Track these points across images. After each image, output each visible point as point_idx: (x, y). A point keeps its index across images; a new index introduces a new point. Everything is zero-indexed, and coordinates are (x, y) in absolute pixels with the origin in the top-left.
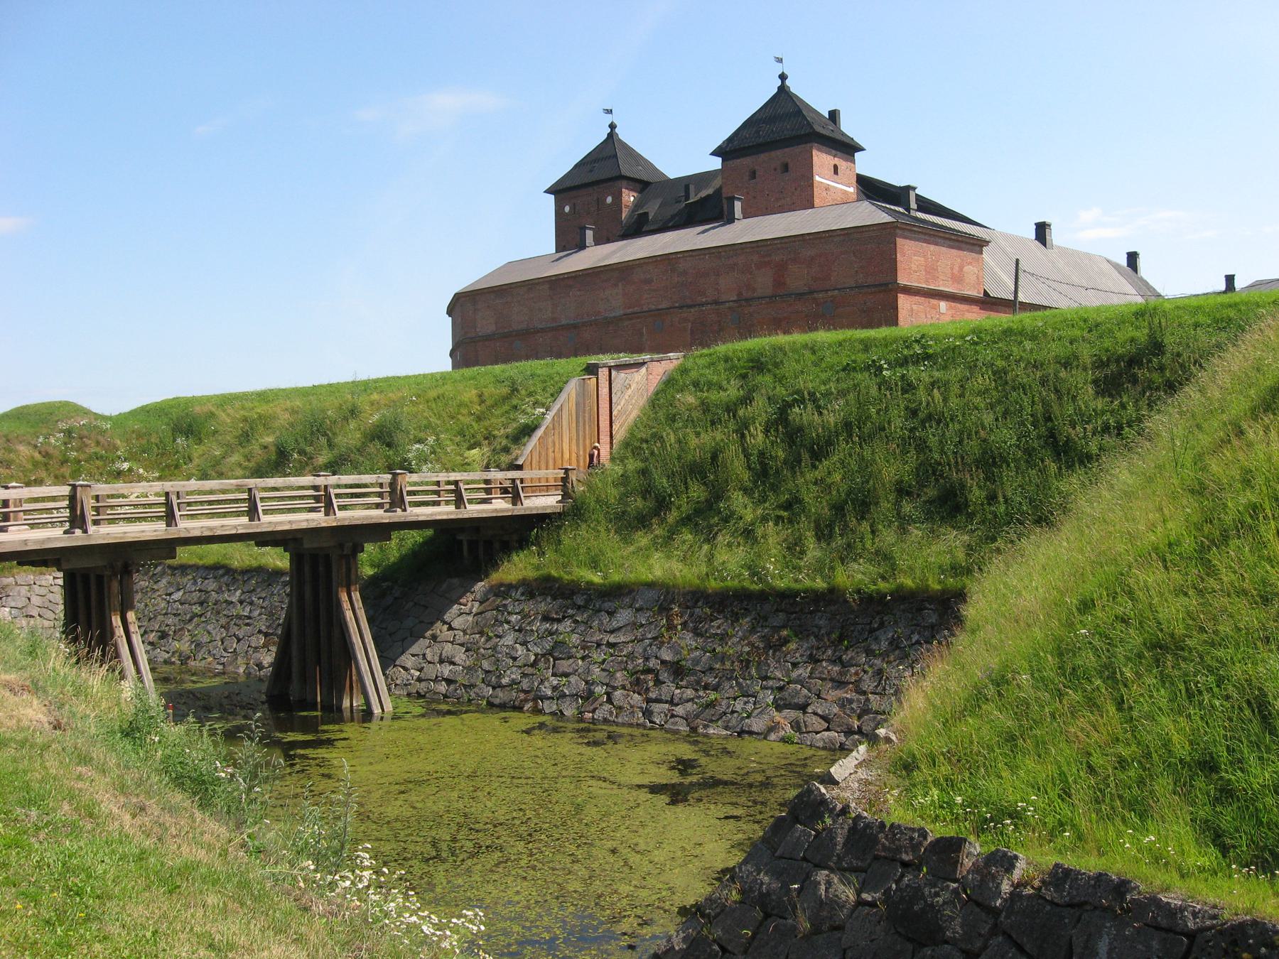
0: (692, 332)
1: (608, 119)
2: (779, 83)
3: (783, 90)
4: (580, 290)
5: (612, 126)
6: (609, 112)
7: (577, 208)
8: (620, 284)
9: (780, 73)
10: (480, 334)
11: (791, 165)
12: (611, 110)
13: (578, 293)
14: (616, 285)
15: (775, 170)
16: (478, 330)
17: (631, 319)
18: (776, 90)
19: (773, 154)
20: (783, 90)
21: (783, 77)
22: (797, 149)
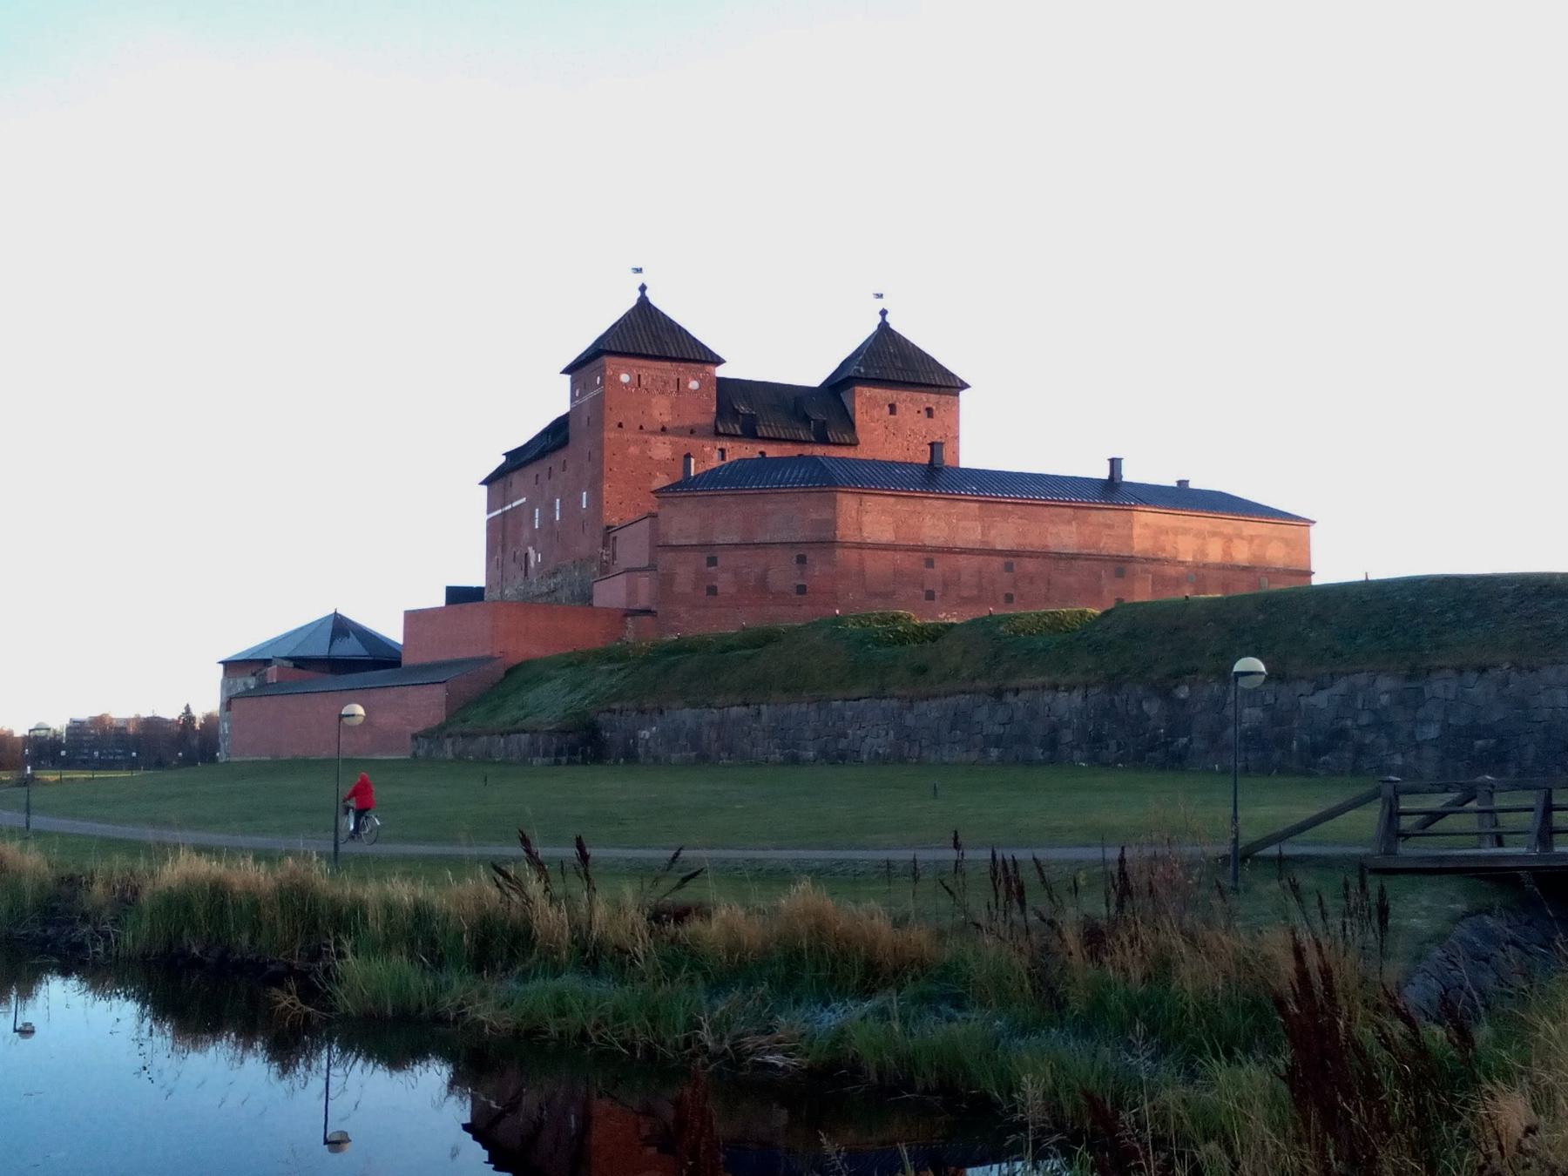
0: (1153, 582)
1: (639, 280)
2: (879, 319)
3: (884, 328)
4: (1020, 518)
5: (643, 288)
6: (639, 271)
7: (643, 382)
8: (1074, 523)
9: (881, 309)
10: (869, 541)
11: (936, 413)
12: (641, 269)
13: (1020, 521)
14: (1069, 522)
15: (919, 412)
16: (865, 535)
17: (1087, 559)
18: (875, 328)
19: (917, 395)
20: (884, 328)
21: (884, 313)
22: (944, 399)
